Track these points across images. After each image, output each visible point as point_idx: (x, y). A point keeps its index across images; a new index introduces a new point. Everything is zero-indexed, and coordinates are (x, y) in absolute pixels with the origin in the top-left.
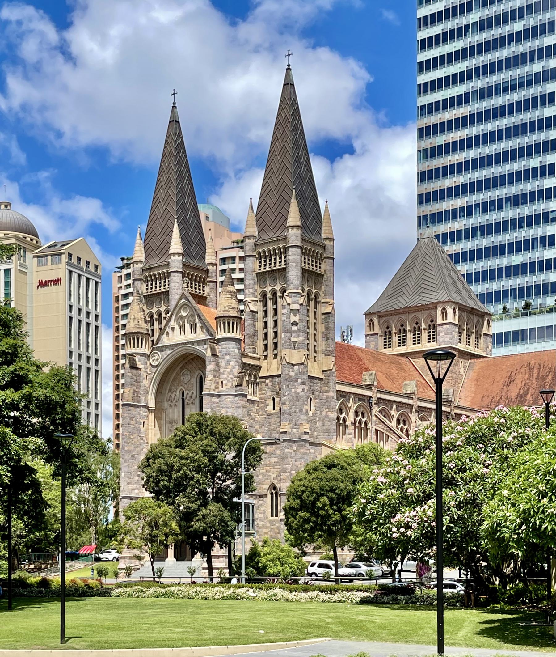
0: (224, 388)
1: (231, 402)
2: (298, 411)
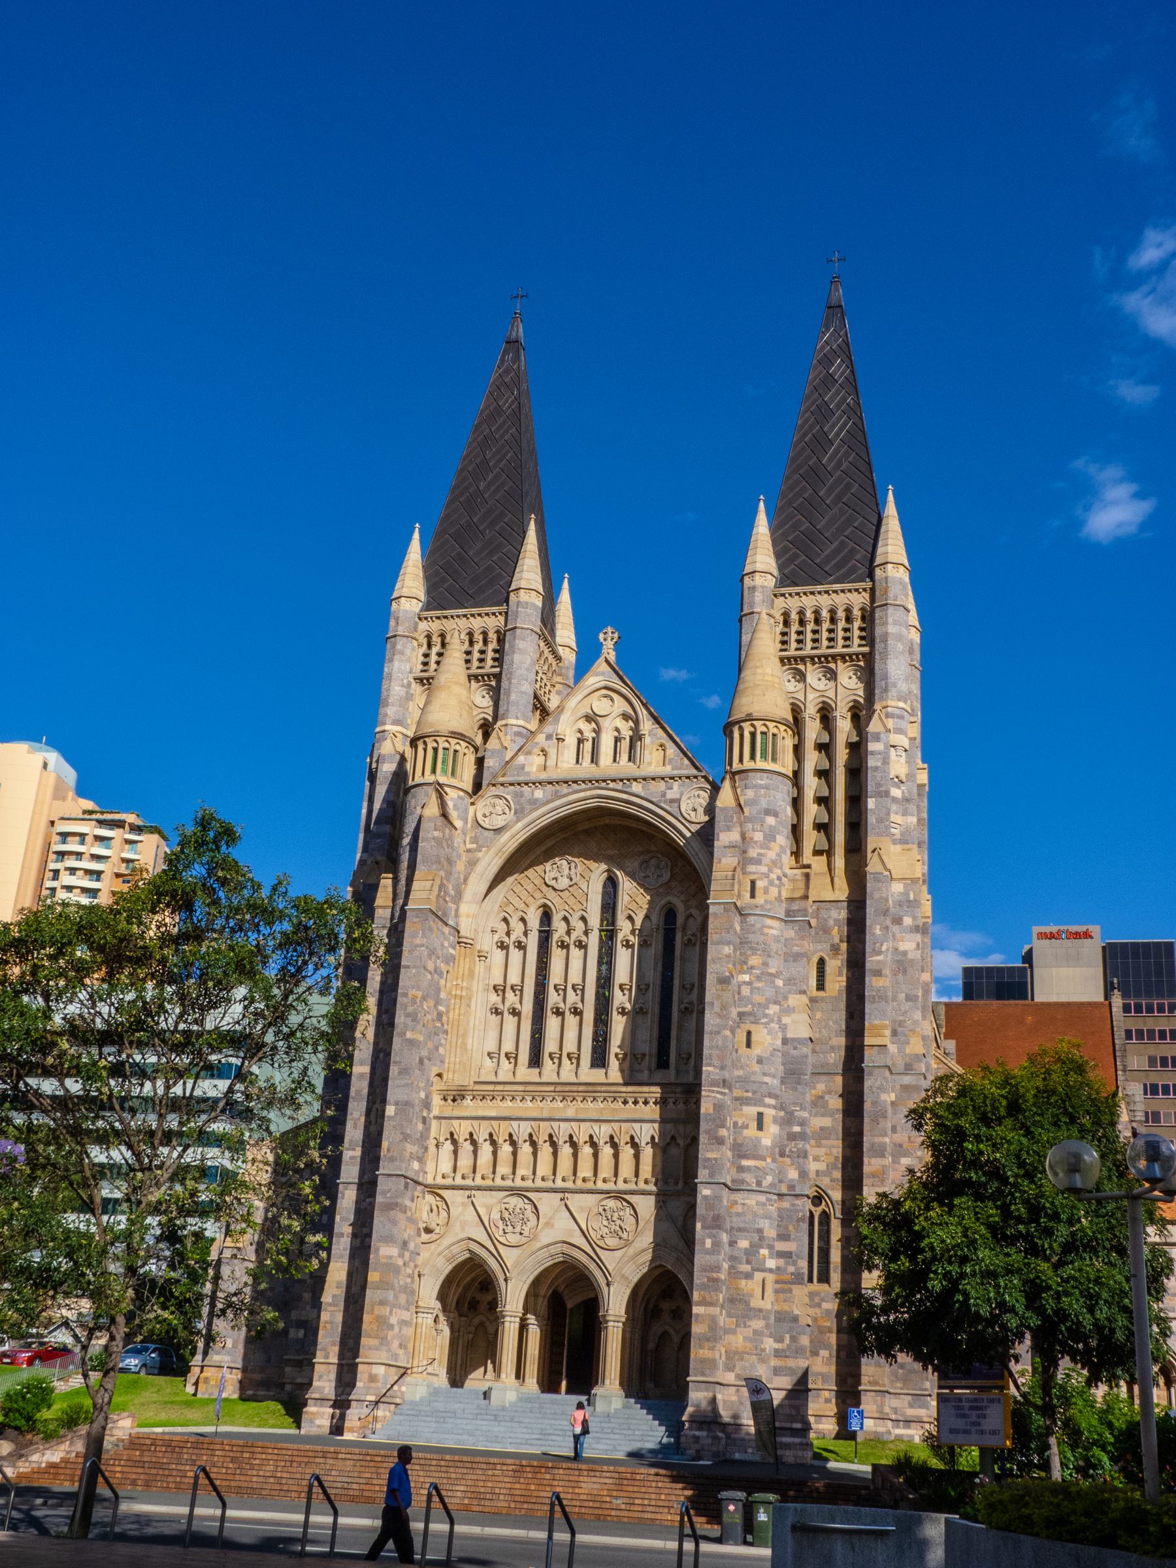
0: (760, 899)
1: (777, 939)
2: (902, 996)
